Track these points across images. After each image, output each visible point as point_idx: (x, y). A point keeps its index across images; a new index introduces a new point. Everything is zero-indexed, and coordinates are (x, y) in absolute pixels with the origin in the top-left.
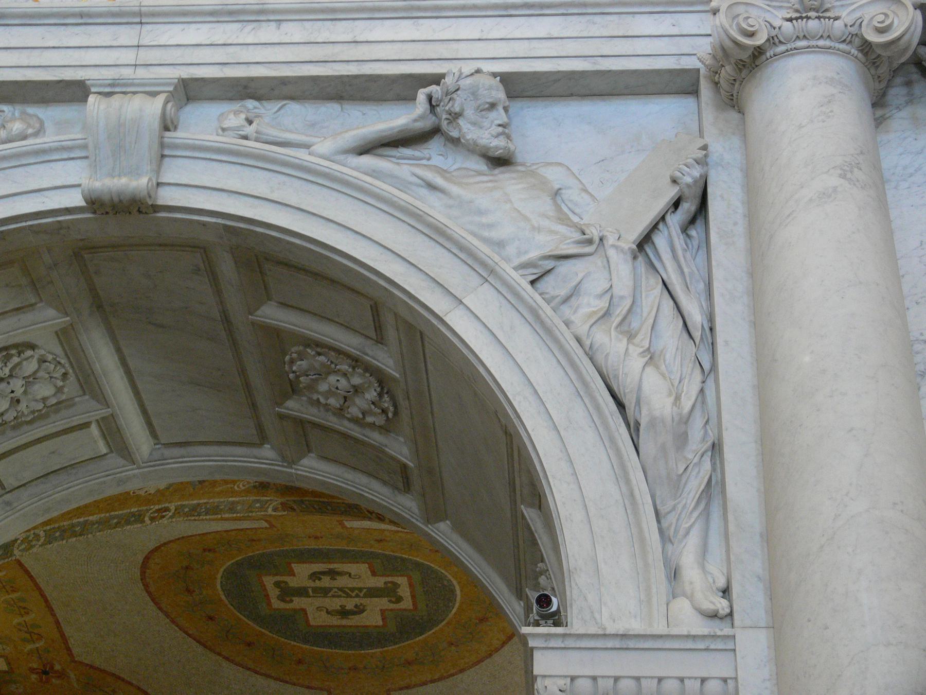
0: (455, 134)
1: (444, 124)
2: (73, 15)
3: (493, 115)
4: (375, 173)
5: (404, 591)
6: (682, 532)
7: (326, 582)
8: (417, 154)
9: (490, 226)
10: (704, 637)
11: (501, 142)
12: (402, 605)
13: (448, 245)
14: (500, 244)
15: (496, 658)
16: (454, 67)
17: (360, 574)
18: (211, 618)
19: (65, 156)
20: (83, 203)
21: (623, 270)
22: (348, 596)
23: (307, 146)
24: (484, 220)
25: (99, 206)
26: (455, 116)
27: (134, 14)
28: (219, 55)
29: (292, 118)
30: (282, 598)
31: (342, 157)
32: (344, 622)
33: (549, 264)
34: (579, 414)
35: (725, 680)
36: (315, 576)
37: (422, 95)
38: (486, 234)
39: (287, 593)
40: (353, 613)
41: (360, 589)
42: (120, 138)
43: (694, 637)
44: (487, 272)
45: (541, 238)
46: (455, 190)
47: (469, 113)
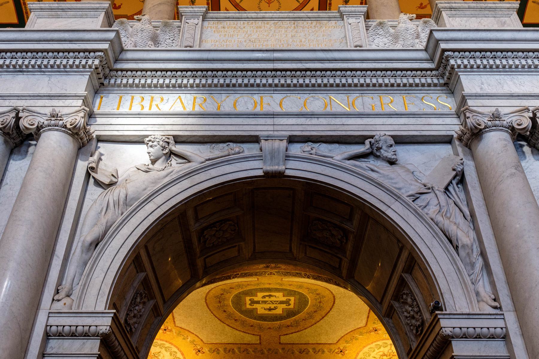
0: (378, 154)
1: (375, 151)
2: (252, 115)
3: (391, 148)
4: (355, 166)
5: (292, 302)
6: (477, 281)
7: (267, 299)
8: (366, 160)
9: (396, 183)
10: (494, 314)
11: (394, 157)
12: (290, 307)
13: (383, 189)
14: (399, 189)
15: (318, 324)
16: (378, 133)
17: (279, 296)
18: (225, 311)
19: (253, 159)
20: (263, 174)
21: (442, 197)
22: (273, 304)
23: (332, 157)
24: (393, 181)
25: (268, 175)
26: (379, 149)
27: (271, 115)
28: (300, 128)
29: (324, 149)
30: (250, 305)
31: (344, 161)
32: (269, 312)
33: (418, 195)
34: (435, 242)
35: (502, 328)
36: (264, 297)
37: (367, 142)
38: (394, 186)
39: (253, 302)
40: (273, 309)
41: (277, 301)
42: (273, 154)
43: (491, 314)
44: (397, 198)
45: (413, 187)
46: (381, 171)
47: (384, 147)
